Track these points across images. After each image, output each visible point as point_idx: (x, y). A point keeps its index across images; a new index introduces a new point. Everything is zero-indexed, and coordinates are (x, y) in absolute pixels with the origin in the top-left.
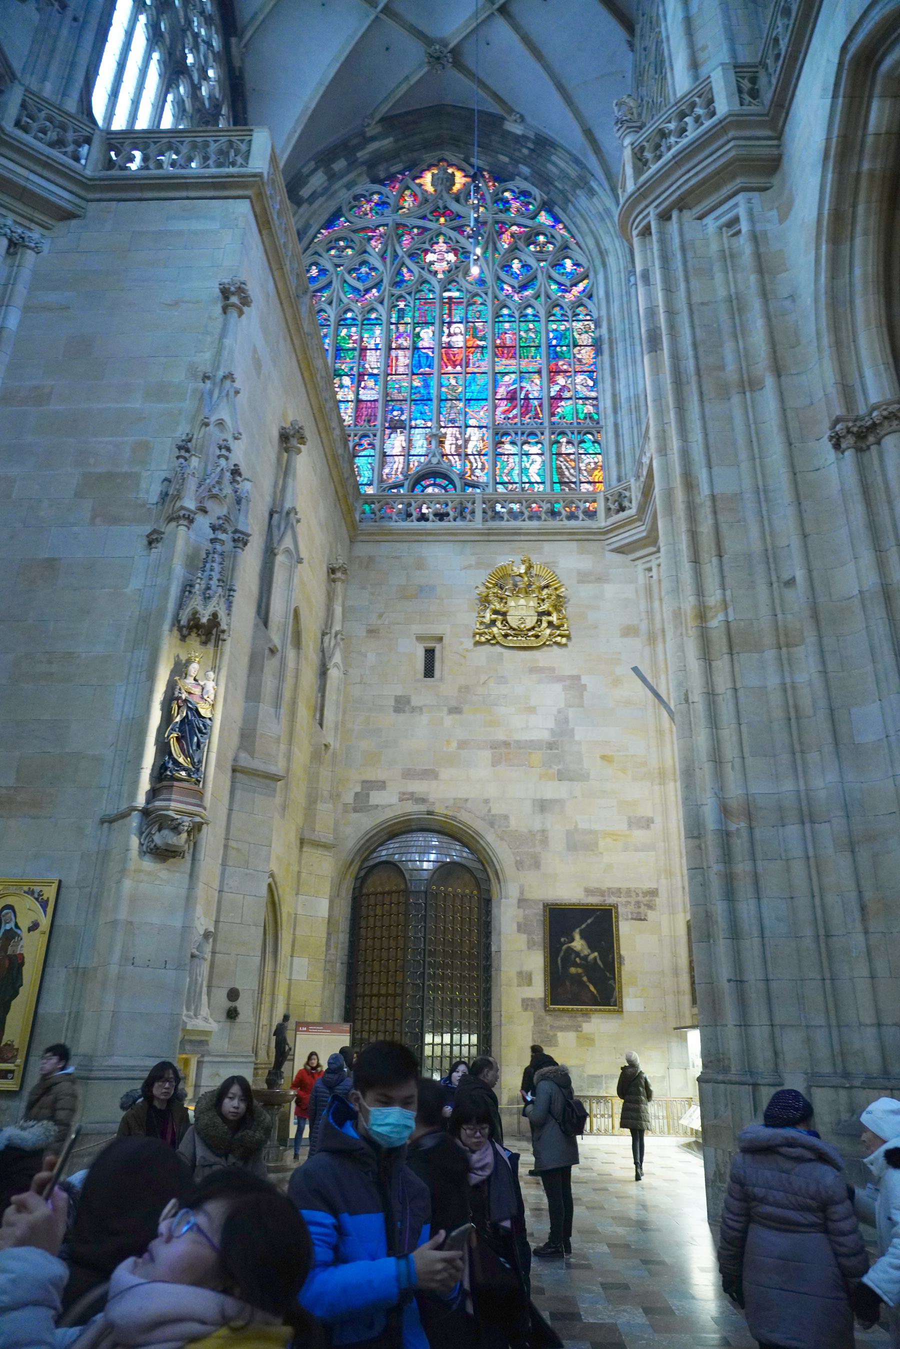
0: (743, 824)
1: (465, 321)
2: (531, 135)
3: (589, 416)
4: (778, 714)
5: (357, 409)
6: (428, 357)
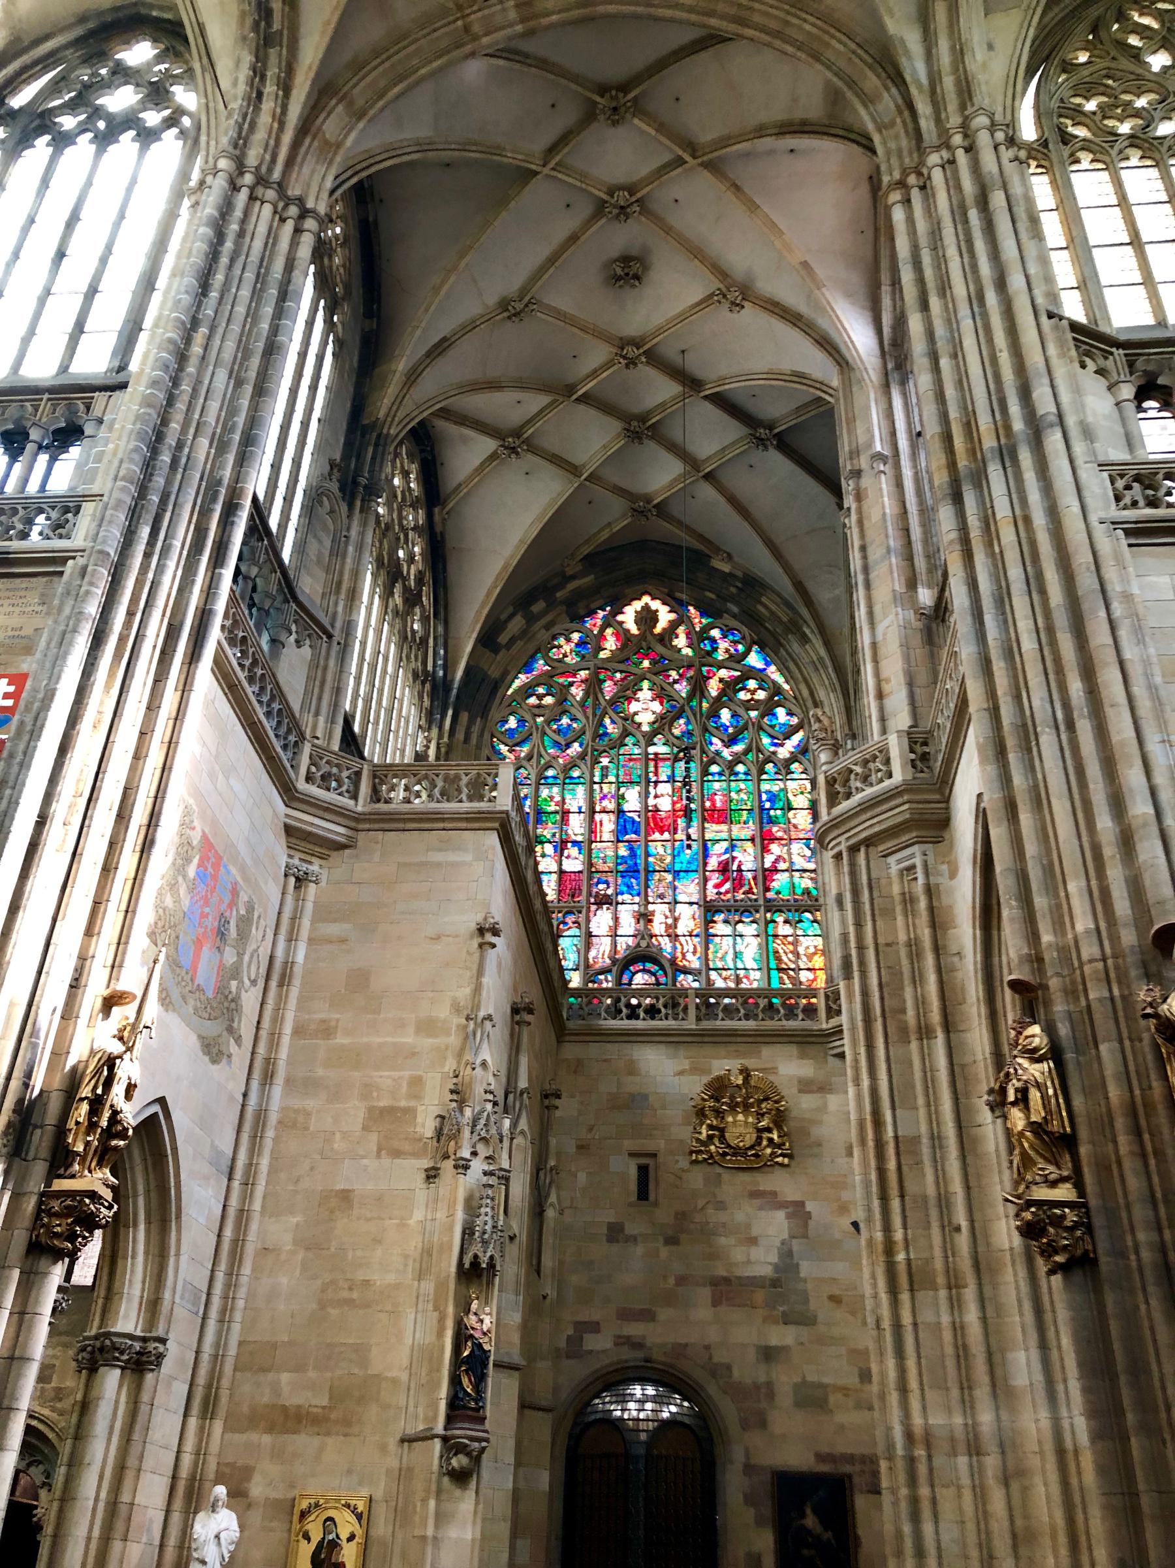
0: (923, 1453)
1: (671, 779)
2: (740, 574)
3: (807, 892)
4: (949, 1350)
5: (560, 882)
6: (634, 821)
